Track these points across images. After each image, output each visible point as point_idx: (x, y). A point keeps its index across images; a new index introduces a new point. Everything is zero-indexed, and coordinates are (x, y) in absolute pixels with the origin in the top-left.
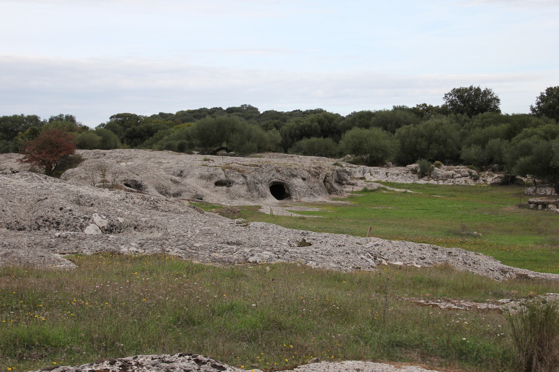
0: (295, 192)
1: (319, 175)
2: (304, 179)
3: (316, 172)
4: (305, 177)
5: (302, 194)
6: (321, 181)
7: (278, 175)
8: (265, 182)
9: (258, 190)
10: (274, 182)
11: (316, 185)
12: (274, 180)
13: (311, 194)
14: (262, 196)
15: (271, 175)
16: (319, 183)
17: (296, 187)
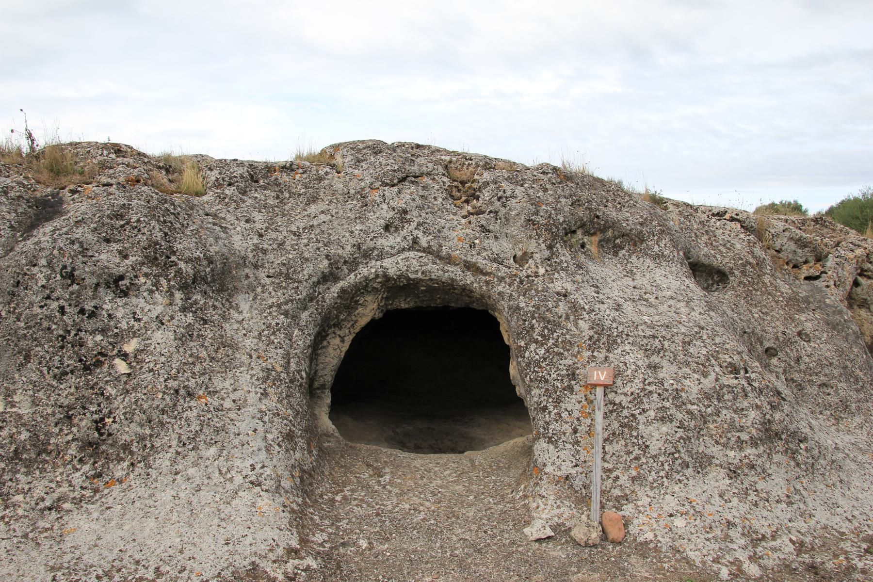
0: (572, 403)
1: (820, 259)
2: (706, 274)
3: (801, 243)
4: (719, 261)
5: (657, 435)
6: (835, 297)
7: (456, 231)
8: (286, 275)
9: (90, 366)
10: (395, 286)
11: (808, 321)
12: (392, 266)
13: (769, 434)
14: (97, 447)
15: (385, 213)
16: (822, 306)
17: (604, 339)
